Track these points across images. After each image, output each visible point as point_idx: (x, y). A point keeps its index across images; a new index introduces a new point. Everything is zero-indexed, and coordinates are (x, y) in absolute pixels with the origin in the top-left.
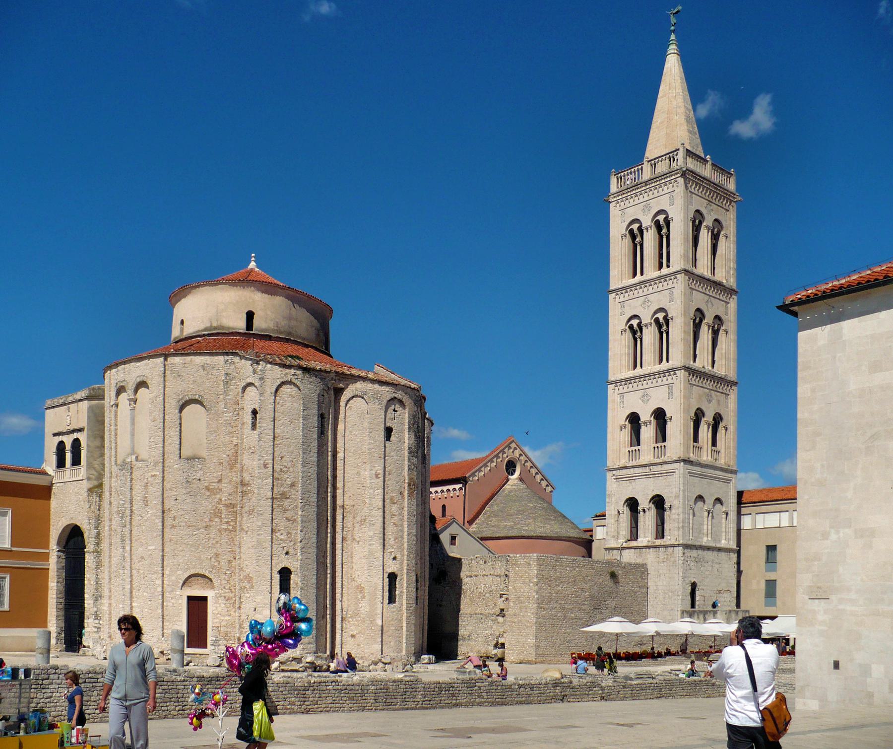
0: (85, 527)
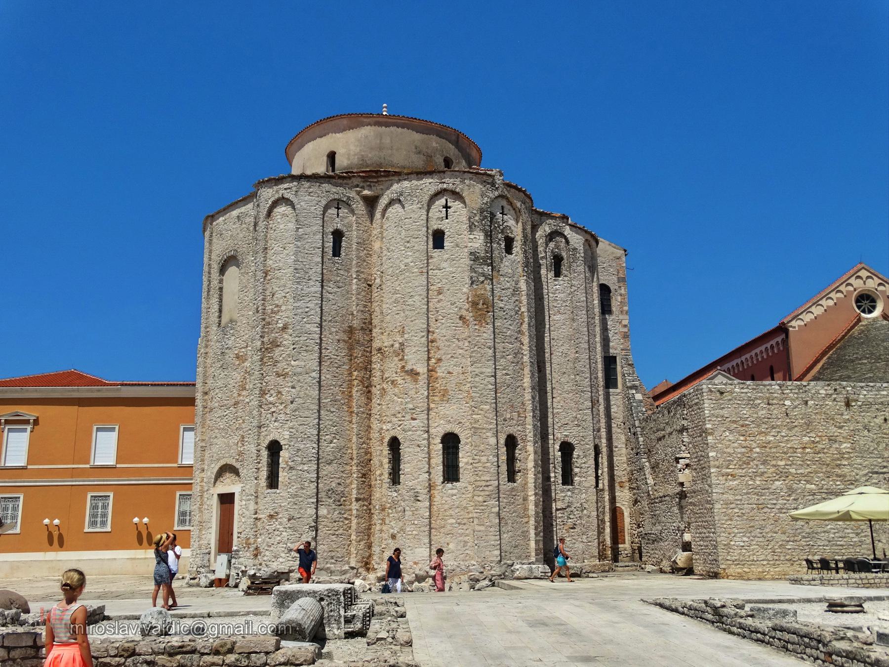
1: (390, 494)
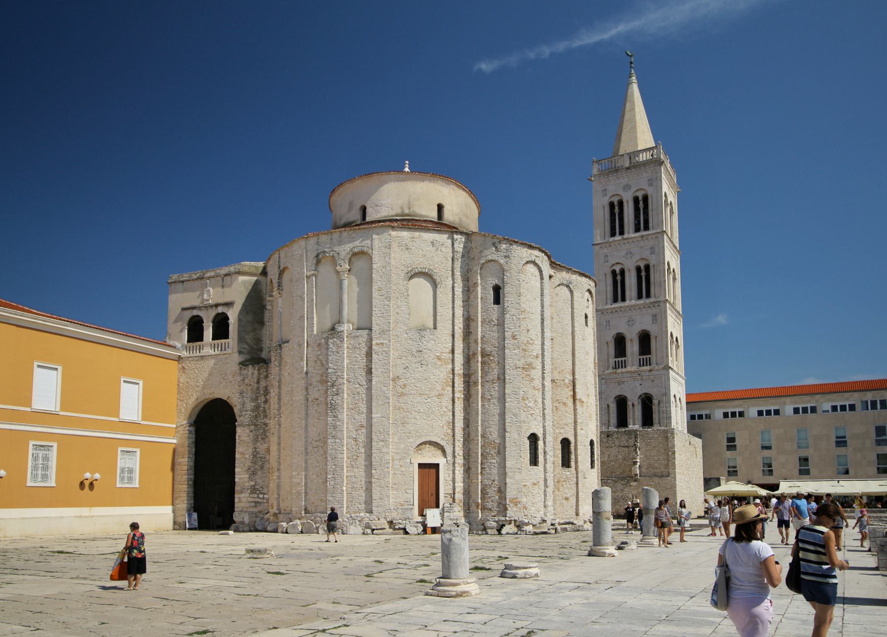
0: (235, 401)
1: (563, 473)
